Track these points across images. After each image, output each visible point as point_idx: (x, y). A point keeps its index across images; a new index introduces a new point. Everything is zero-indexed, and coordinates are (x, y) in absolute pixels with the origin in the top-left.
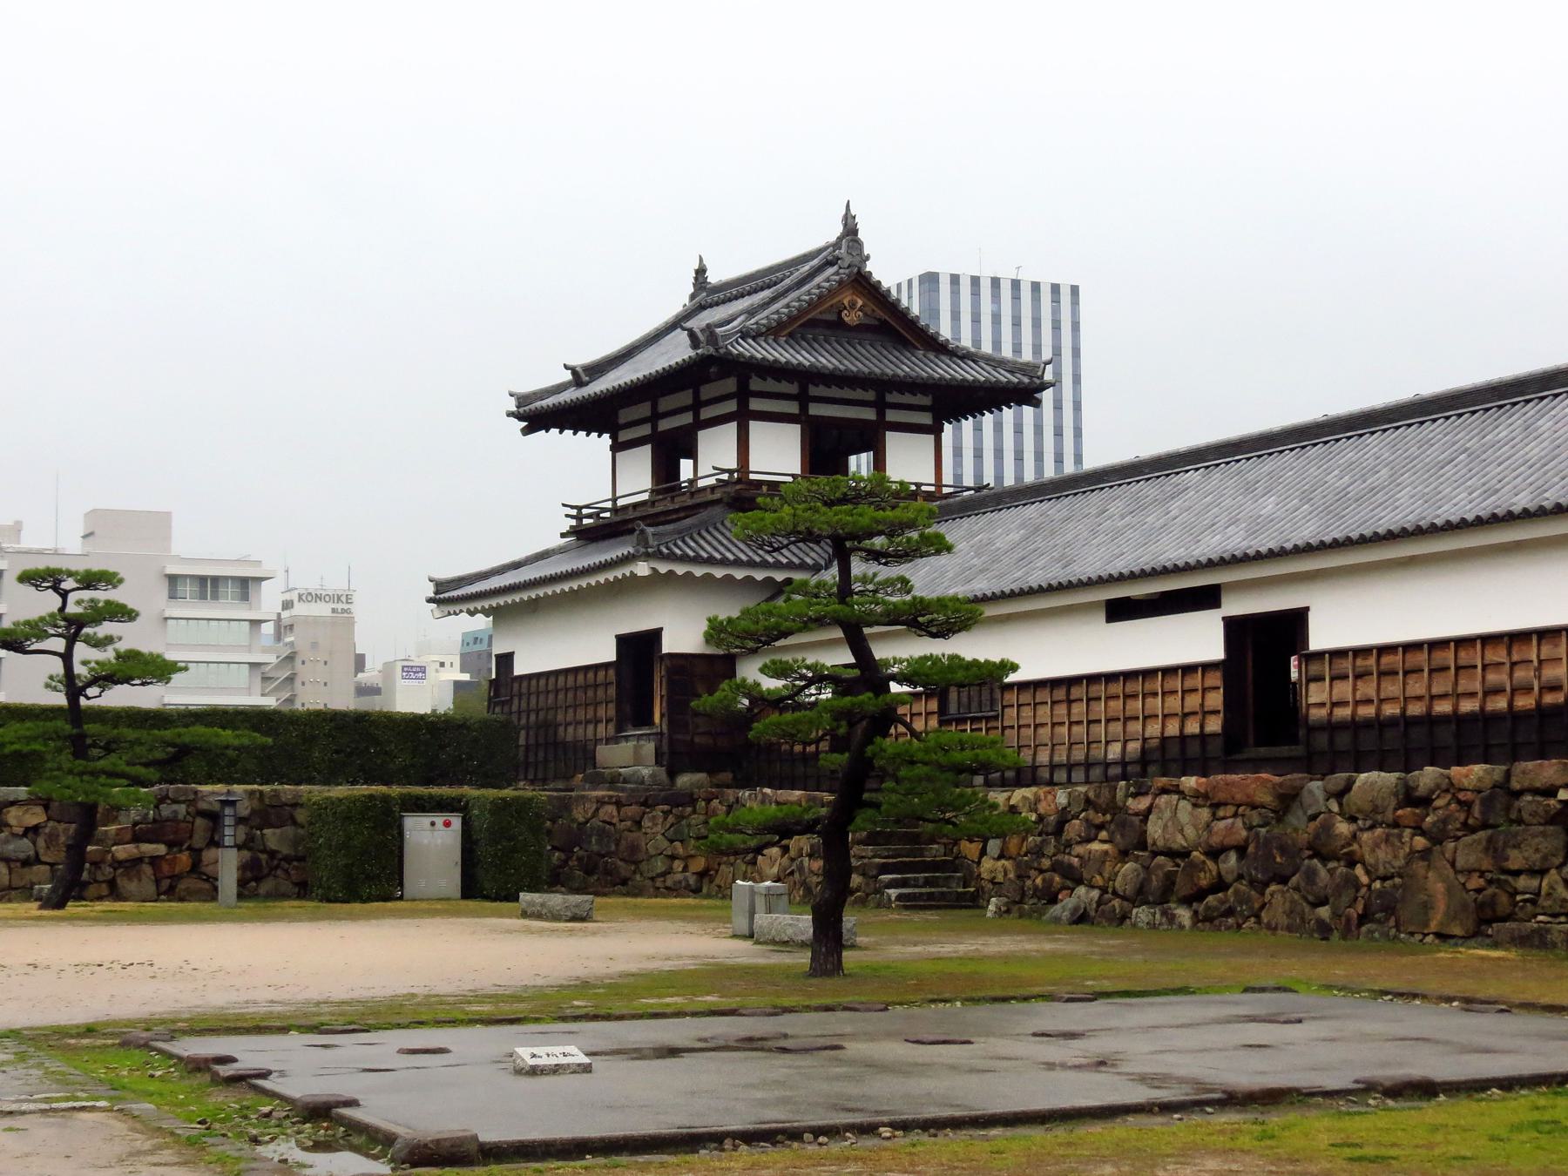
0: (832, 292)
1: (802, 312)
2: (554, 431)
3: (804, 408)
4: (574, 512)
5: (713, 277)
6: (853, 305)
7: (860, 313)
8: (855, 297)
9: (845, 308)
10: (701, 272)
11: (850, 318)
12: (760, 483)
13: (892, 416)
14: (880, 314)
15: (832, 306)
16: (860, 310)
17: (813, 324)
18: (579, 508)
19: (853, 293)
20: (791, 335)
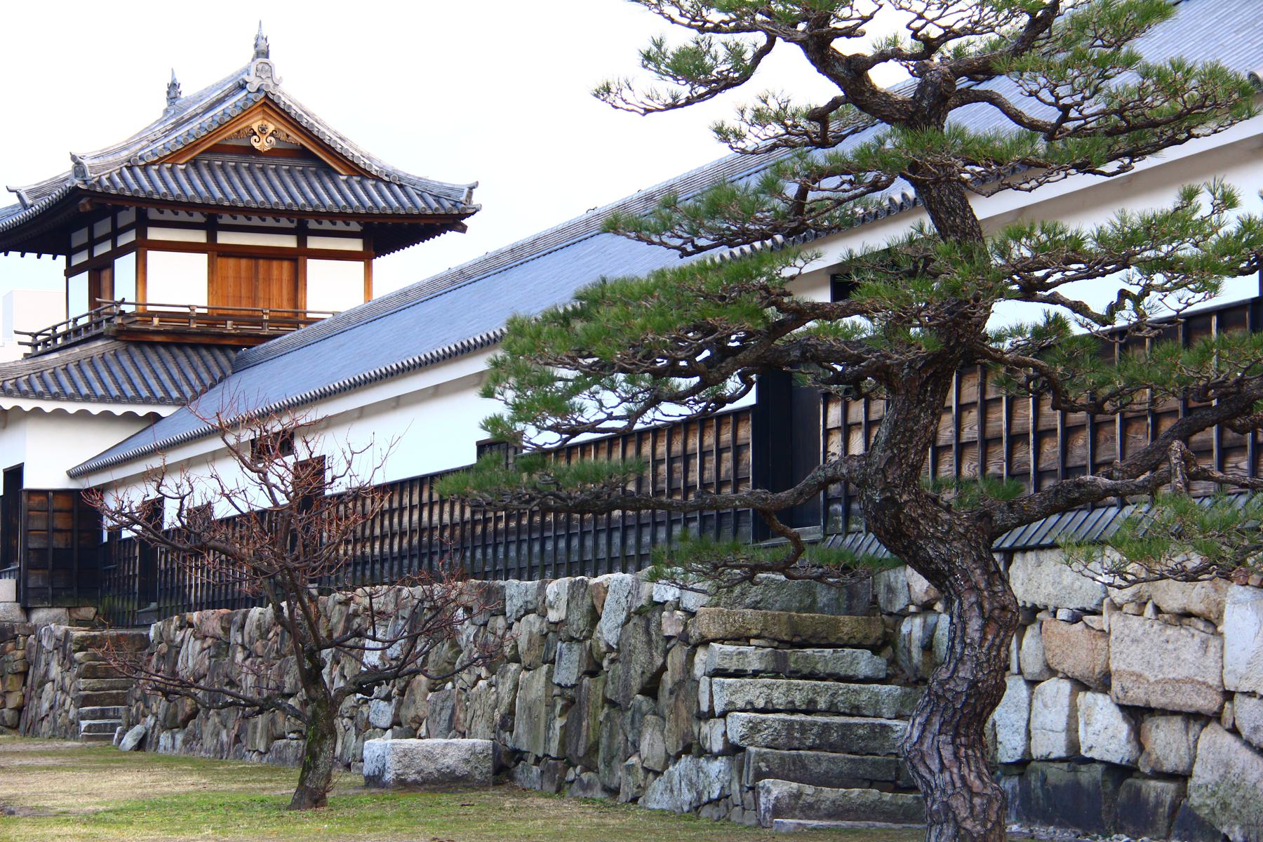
0: (234, 120)
1: (211, 134)
2: (14, 255)
3: (212, 237)
4: (29, 339)
5: (188, 90)
6: (263, 130)
7: (272, 139)
8: (266, 122)
9: (255, 134)
10: (174, 86)
11: (262, 144)
12: (153, 314)
13: (314, 243)
14: (296, 139)
15: (239, 132)
16: (272, 135)
17: (218, 149)
18: (35, 335)
19: (264, 119)
20: (194, 163)
